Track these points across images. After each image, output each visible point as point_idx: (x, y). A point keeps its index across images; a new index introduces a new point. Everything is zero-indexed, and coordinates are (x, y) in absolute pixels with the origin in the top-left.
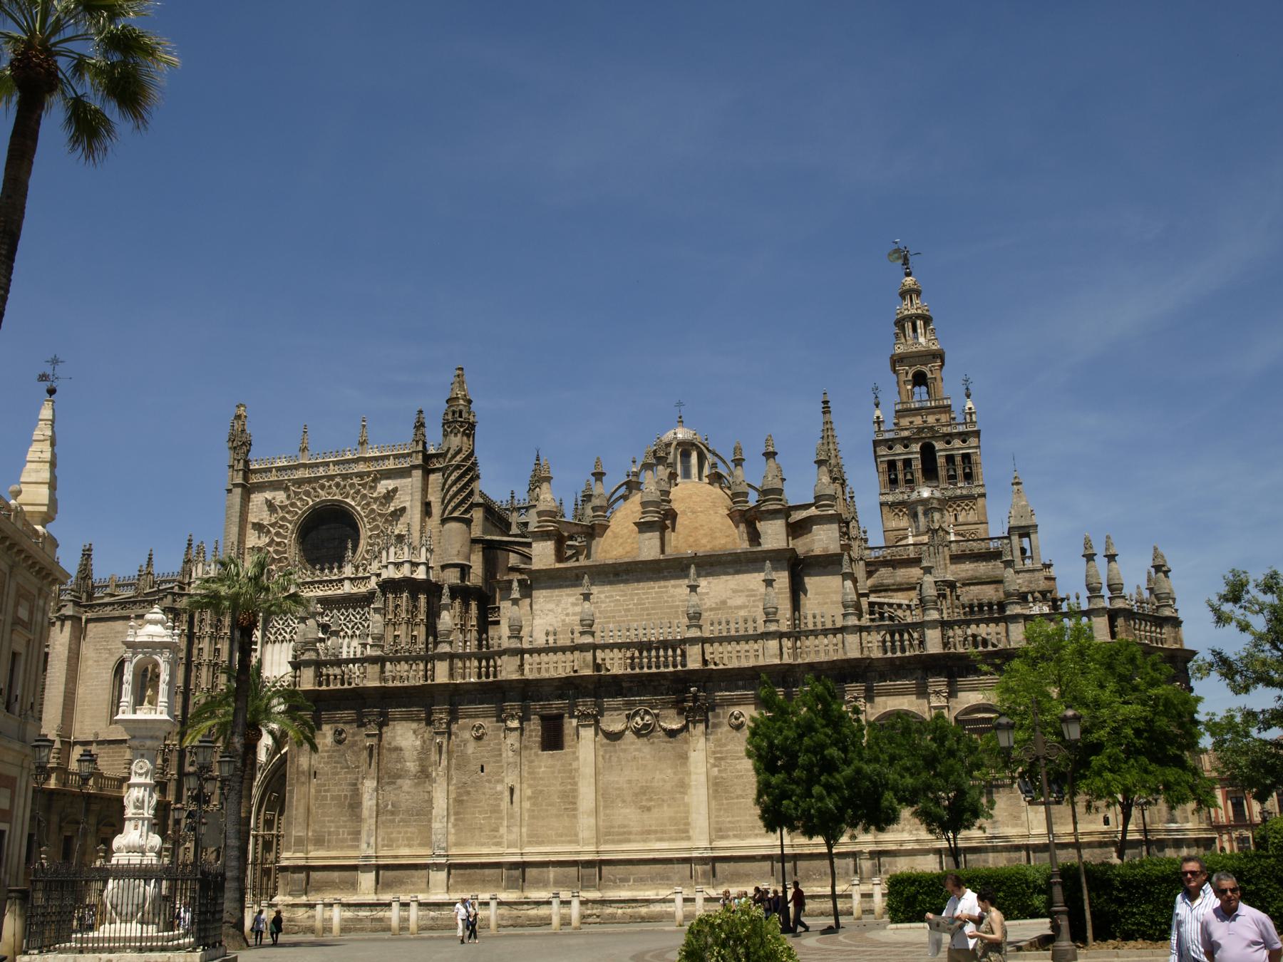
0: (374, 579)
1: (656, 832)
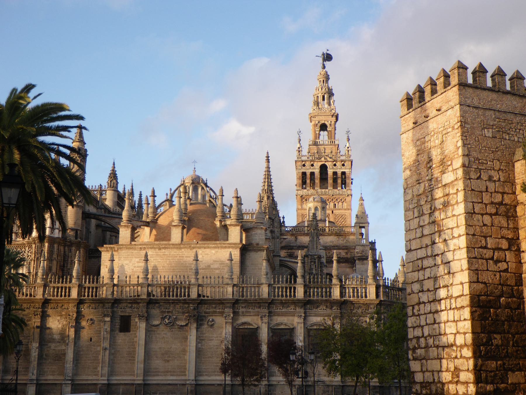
1: (170, 372)
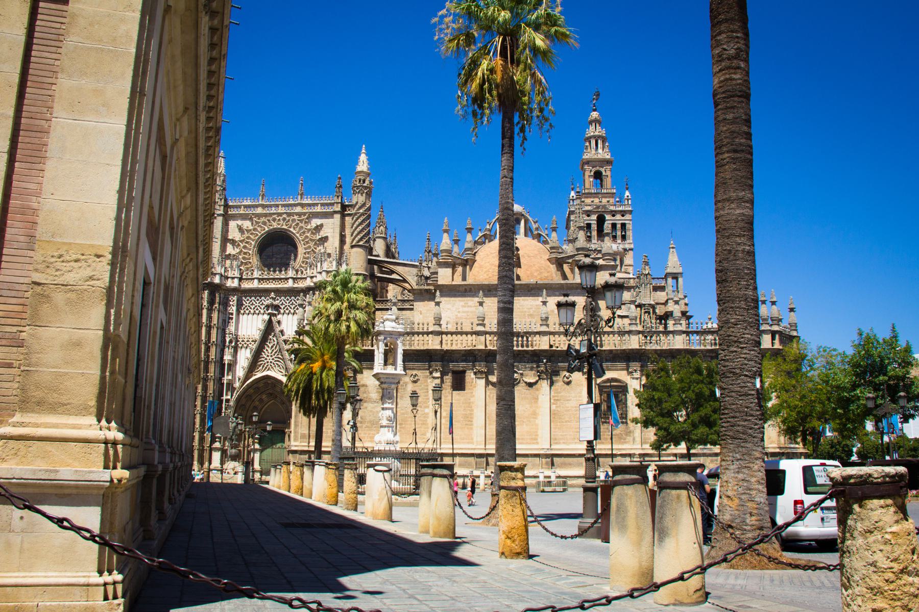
0: (309, 279)
